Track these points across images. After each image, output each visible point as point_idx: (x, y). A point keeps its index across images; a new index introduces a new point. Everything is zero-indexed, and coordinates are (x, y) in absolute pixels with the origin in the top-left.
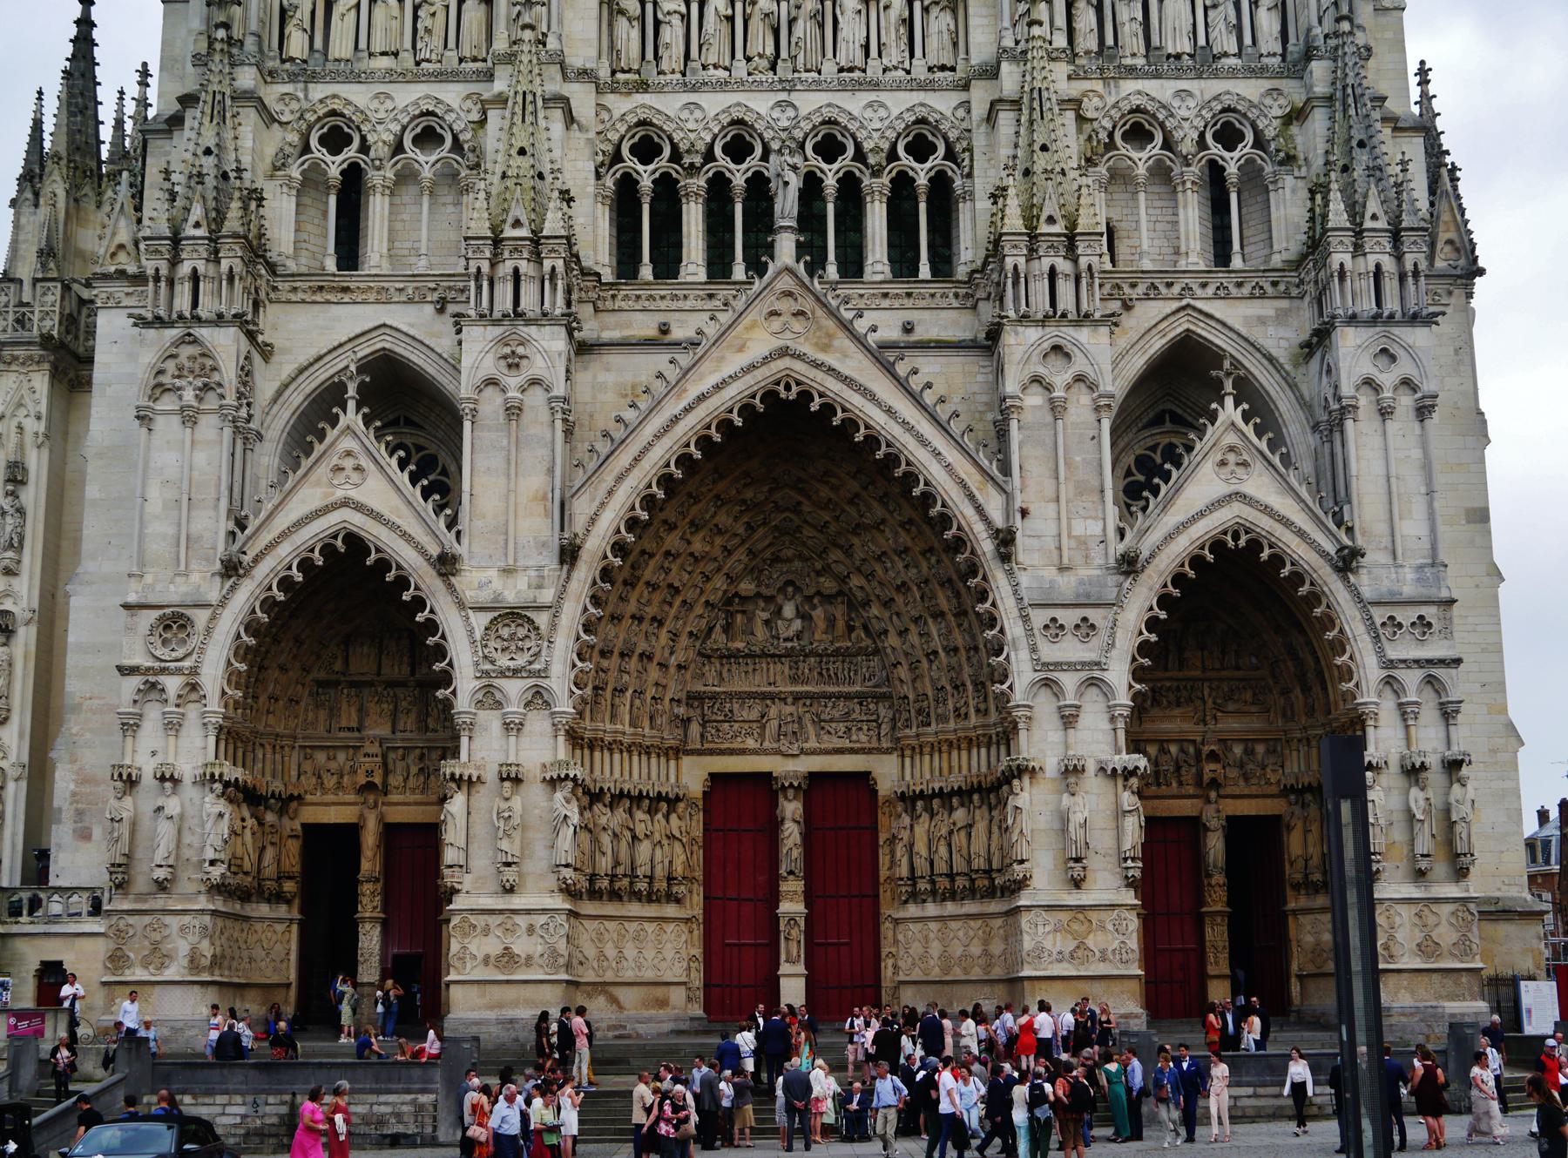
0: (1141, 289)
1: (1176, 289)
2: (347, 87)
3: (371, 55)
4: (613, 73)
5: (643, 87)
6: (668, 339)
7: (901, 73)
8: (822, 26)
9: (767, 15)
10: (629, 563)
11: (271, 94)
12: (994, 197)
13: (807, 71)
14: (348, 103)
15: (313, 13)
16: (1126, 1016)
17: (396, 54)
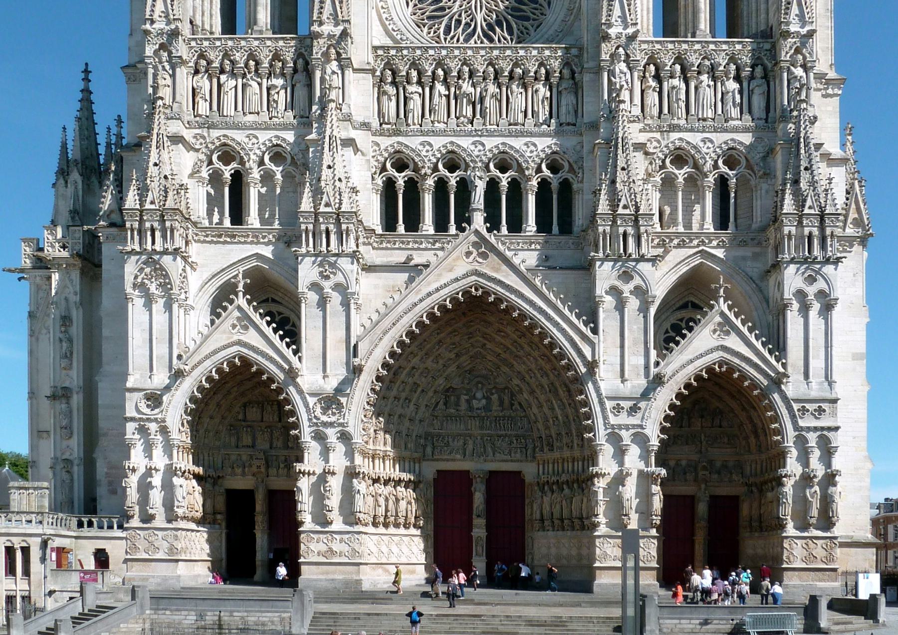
0: (676, 242)
1: (695, 242)
2: (231, 131)
3: (244, 113)
4: (381, 125)
5: (397, 133)
6: (412, 263)
7: (546, 127)
8: (500, 101)
9: (468, 95)
10: (392, 372)
11: (188, 134)
12: (595, 192)
13: (490, 125)
14: (234, 140)
15: (211, 91)
16: (649, 585)
17: (258, 113)
